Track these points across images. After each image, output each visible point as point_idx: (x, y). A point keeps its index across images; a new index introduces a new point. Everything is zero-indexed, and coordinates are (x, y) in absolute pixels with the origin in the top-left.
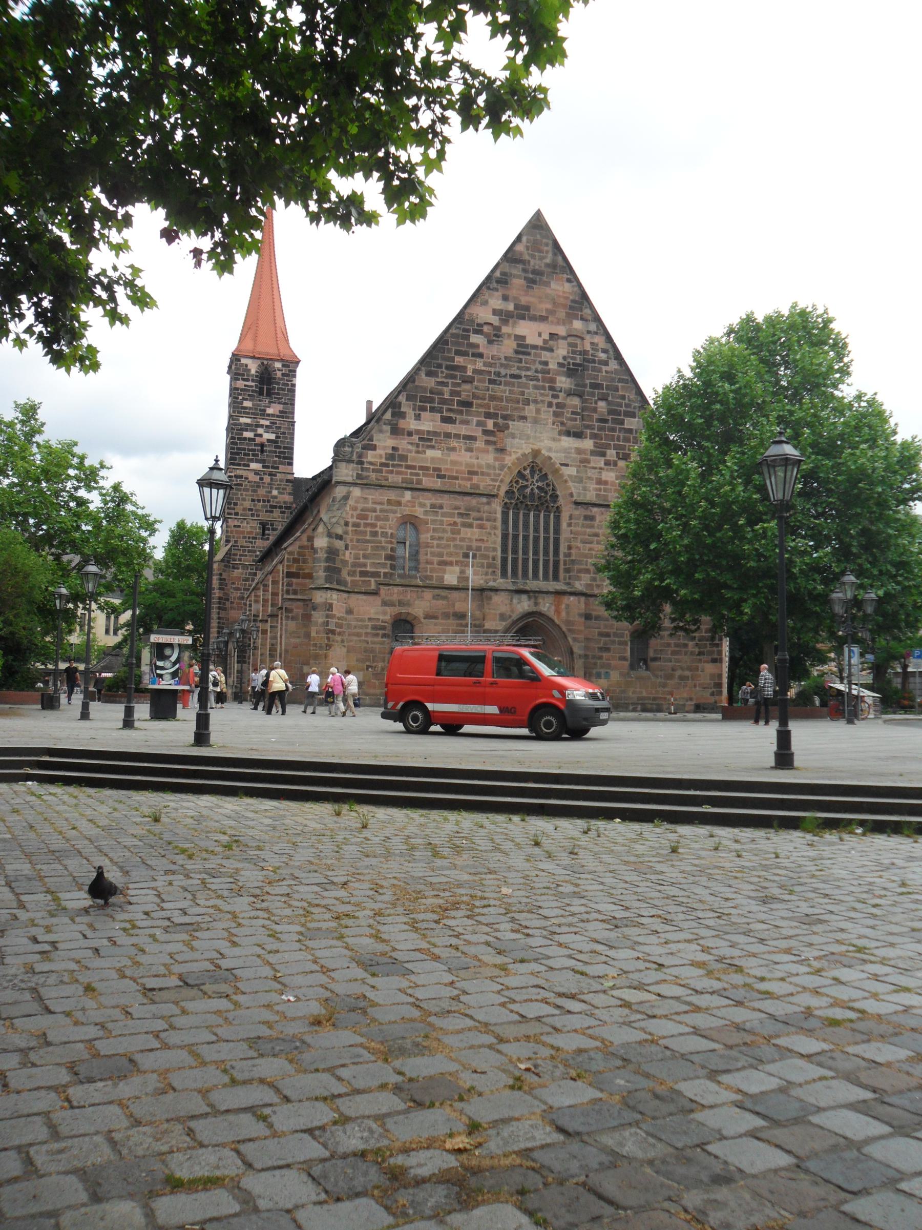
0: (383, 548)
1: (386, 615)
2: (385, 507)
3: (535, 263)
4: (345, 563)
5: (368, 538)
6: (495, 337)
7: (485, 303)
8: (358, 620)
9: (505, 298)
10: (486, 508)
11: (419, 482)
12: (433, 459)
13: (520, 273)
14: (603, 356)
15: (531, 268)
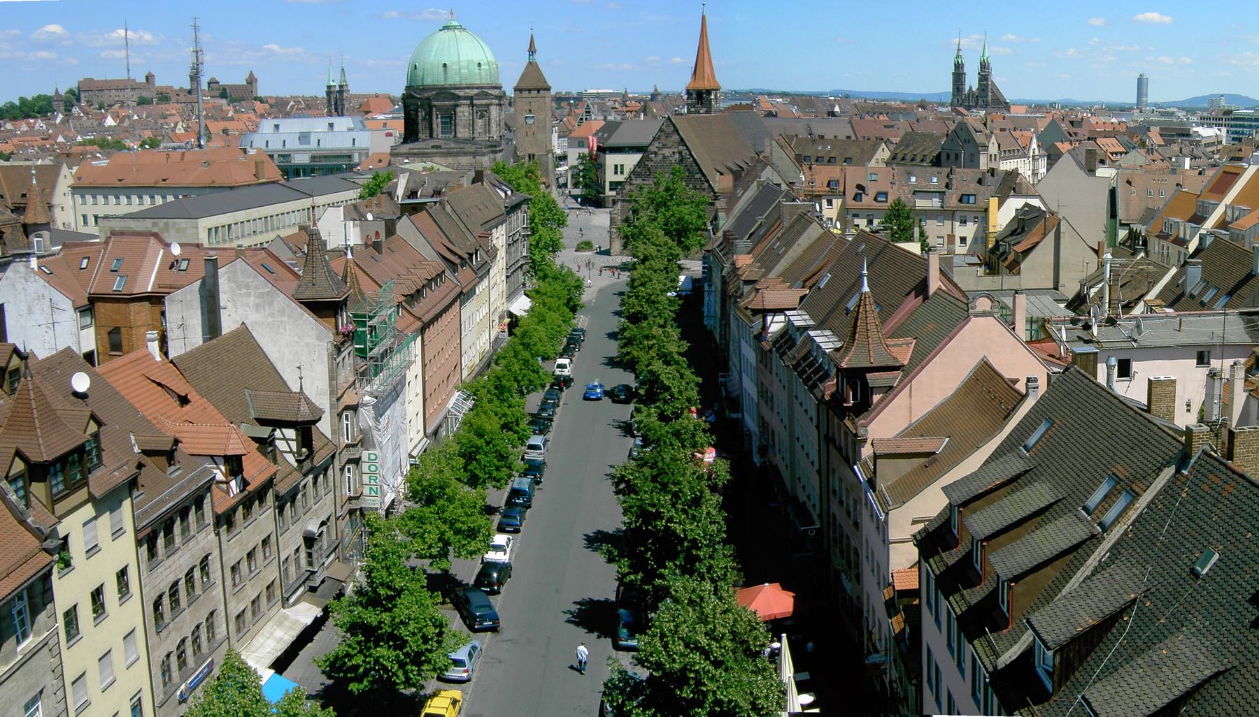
3: (668, 131)
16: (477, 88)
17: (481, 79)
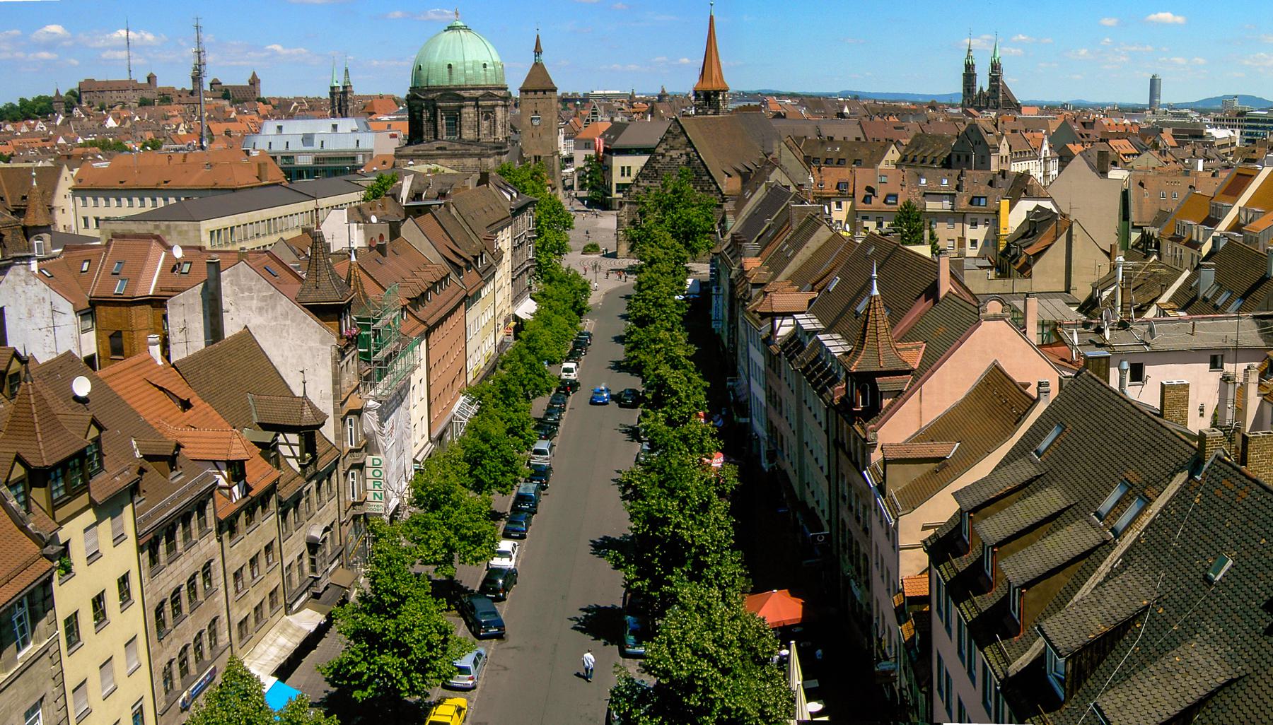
16: (483, 89)
17: (486, 80)
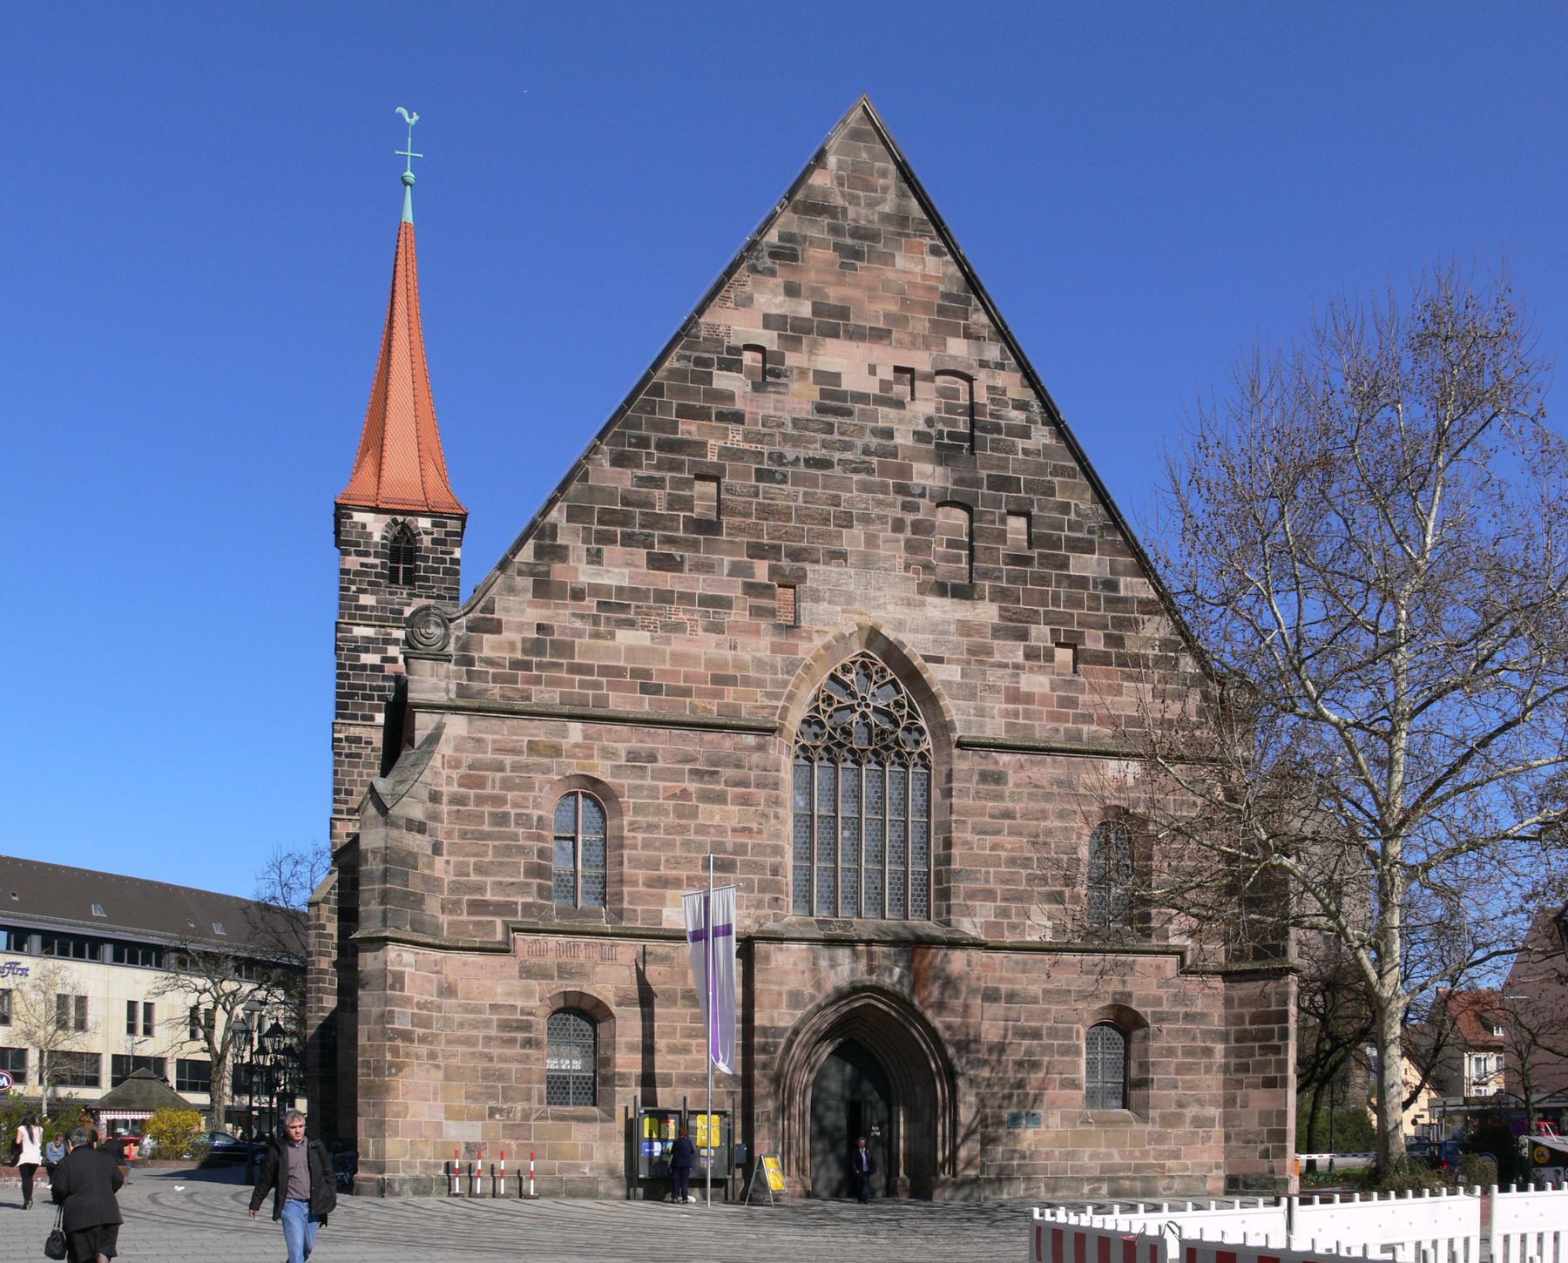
0: (522, 850)
1: (536, 1000)
2: (524, 759)
3: (859, 214)
4: (433, 884)
5: (486, 828)
6: (770, 374)
7: (747, 302)
8: (466, 1009)
9: (792, 291)
10: (756, 758)
11: (602, 701)
12: (631, 651)
13: (826, 236)
14: (1018, 417)
15: (848, 224)
